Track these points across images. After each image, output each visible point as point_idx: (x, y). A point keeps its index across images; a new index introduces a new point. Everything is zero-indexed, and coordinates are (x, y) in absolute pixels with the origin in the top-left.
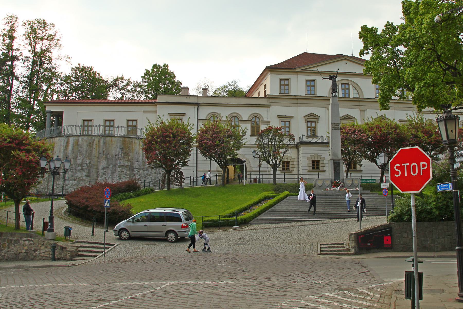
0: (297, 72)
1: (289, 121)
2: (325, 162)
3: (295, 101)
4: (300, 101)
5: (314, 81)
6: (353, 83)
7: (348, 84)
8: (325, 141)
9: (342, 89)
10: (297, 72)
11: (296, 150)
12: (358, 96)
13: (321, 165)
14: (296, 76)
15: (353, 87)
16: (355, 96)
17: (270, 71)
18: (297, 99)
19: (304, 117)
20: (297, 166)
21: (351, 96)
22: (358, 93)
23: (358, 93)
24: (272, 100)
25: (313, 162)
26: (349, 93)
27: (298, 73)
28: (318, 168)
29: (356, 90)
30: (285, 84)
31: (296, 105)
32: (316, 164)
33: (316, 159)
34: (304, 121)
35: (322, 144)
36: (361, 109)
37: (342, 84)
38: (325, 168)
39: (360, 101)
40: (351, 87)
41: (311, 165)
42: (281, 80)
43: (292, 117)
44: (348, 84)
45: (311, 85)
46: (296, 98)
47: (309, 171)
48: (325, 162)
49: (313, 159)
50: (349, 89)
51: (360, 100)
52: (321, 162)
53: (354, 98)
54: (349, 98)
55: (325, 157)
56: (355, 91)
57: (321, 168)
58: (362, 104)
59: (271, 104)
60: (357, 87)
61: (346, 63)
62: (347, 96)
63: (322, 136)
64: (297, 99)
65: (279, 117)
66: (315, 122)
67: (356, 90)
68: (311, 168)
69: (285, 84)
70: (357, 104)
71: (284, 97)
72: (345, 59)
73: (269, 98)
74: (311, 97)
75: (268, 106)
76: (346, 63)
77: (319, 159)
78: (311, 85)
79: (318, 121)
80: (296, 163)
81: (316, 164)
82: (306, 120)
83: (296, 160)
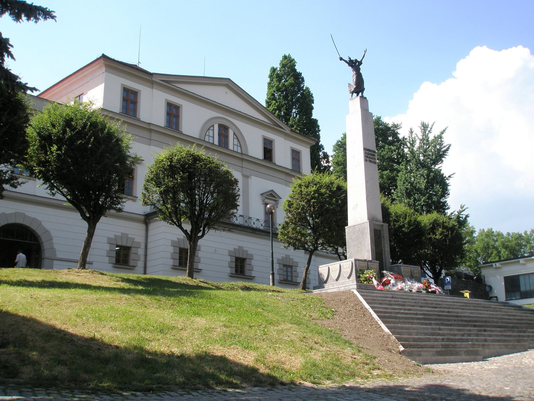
3: (146, 134)
4: (154, 136)
6: (233, 127)
11: (142, 226)
12: (239, 151)
15: (234, 134)
16: (235, 150)
18: (150, 130)
20: (142, 258)
21: (231, 147)
22: (240, 146)
23: (240, 146)
29: (237, 139)
39: (242, 159)
45: (173, 112)
46: (149, 129)
50: (227, 137)
51: (244, 157)
56: (236, 141)
58: (245, 164)
60: (238, 136)
61: (226, 93)
64: (150, 130)
67: (238, 140)
68: (177, 263)
70: (238, 163)
72: (227, 86)
76: (226, 93)
78: (173, 112)
80: (141, 252)
83: (143, 246)
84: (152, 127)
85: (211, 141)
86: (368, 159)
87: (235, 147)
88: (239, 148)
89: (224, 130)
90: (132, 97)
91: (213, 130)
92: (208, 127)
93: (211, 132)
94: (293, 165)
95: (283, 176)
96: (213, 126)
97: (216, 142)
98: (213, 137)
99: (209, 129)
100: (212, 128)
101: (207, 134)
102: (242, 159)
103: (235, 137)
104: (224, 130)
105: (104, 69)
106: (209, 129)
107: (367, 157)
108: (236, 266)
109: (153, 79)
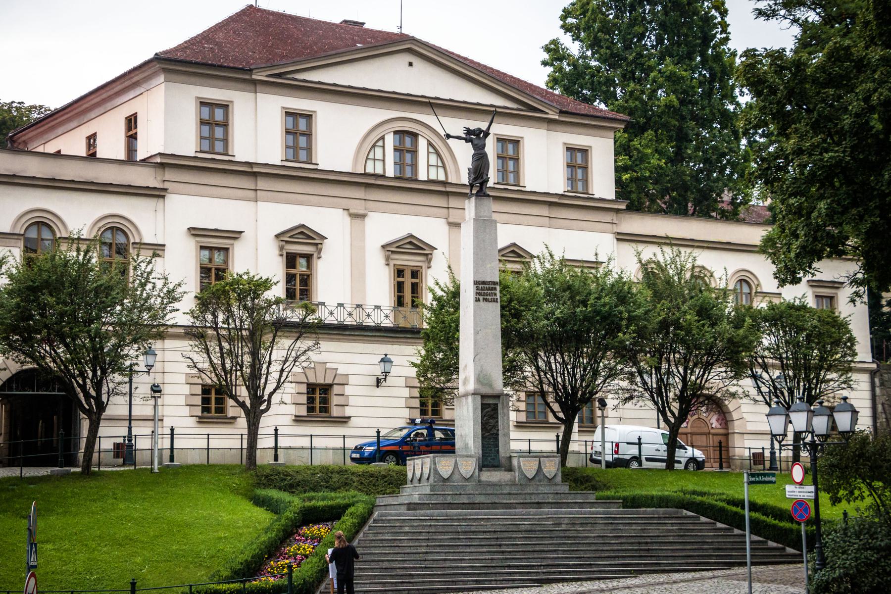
0: (255, 83)
1: (227, 249)
2: (348, 390)
3: (247, 183)
4: (262, 184)
5: (308, 117)
7: (414, 136)
8: (349, 321)
9: (395, 150)
10: (255, 83)
12: (442, 177)
13: (335, 400)
14: (250, 95)
15: (430, 144)
16: (433, 177)
17: (165, 70)
18: (255, 175)
19: (277, 236)
21: (422, 176)
22: (444, 167)
24: (169, 175)
25: (312, 388)
26: (414, 166)
27: (259, 88)
28: (325, 409)
30: (215, 121)
31: (251, 194)
32: (317, 396)
33: (320, 381)
34: (277, 252)
35: (340, 331)
36: (451, 220)
37: (395, 133)
38: (348, 412)
40: (422, 144)
41: (304, 399)
42: (203, 103)
43: (235, 235)
44: (414, 136)
45: (299, 129)
46: (252, 172)
47: (298, 420)
48: (348, 390)
49: (312, 380)
50: (414, 152)
51: (449, 189)
52: (336, 389)
53: (430, 182)
54: (416, 180)
55: (347, 375)
56: (433, 159)
57: (335, 412)
59: (167, 185)
61: (411, 64)
62: (408, 173)
63: (341, 305)
64: (255, 175)
65: (195, 232)
66: (308, 257)
68: (303, 411)
69: (215, 121)
71: (212, 164)
72: (409, 51)
73: (162, 165)
74: (297, 172)
75: (157, 194)
76: (411, 64)
77: (329, 381)
78: (299, 129)
79: (320, 251)
81: (317, 396)
82: (281, 248)
84: (255, 170)
85: (379, 171)
86: (481, 298)
87: (433, 171)
88: (441, 171)
89: (406, 141)
90: (219, 114)
91: (383, 147)
92: (372, 142)
93: (378, 152)
94: (572, 180)
95: (545, 211)
96: (383, 138)
97: (390, 172)
98: (384, 161)
99: (374, 146)
100: (380, 143)
101: (371, 156)
102: (447, 194)
103: (431, 150)
104: (406, 141)
105: (161, 78)
106: (374, 146)
107: (480, 294)
108: (422, 404)
109: (254, 77)
